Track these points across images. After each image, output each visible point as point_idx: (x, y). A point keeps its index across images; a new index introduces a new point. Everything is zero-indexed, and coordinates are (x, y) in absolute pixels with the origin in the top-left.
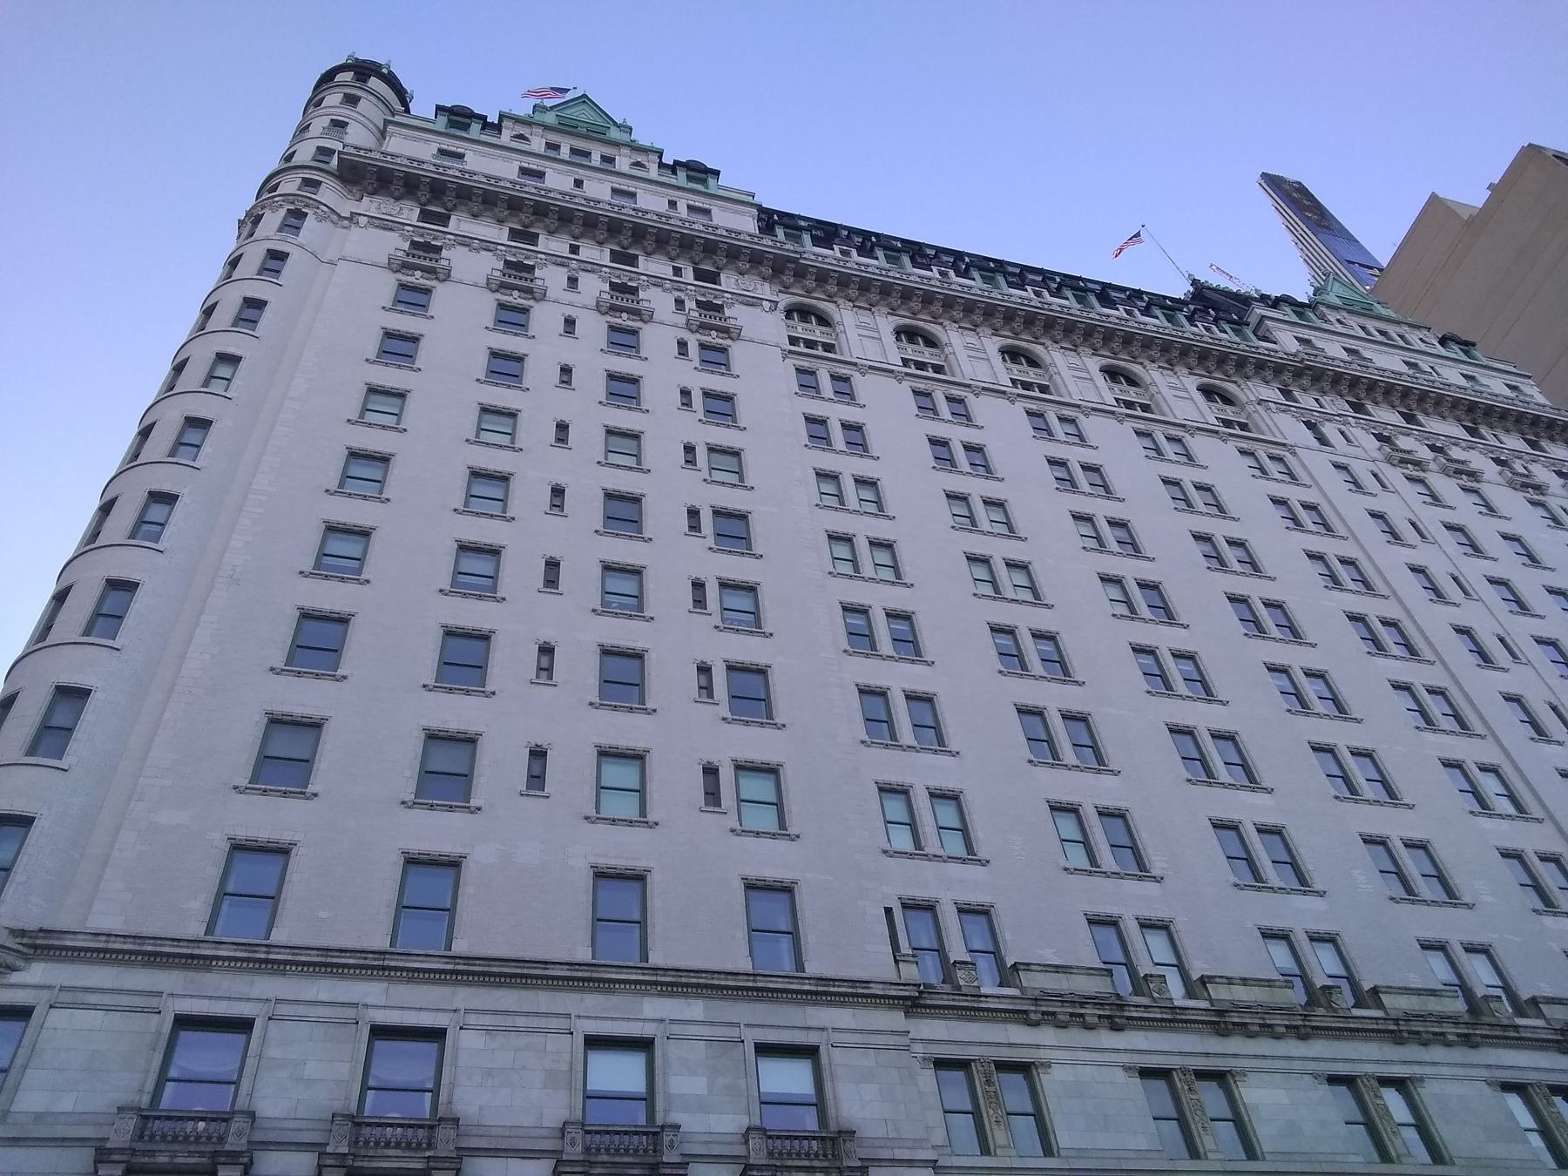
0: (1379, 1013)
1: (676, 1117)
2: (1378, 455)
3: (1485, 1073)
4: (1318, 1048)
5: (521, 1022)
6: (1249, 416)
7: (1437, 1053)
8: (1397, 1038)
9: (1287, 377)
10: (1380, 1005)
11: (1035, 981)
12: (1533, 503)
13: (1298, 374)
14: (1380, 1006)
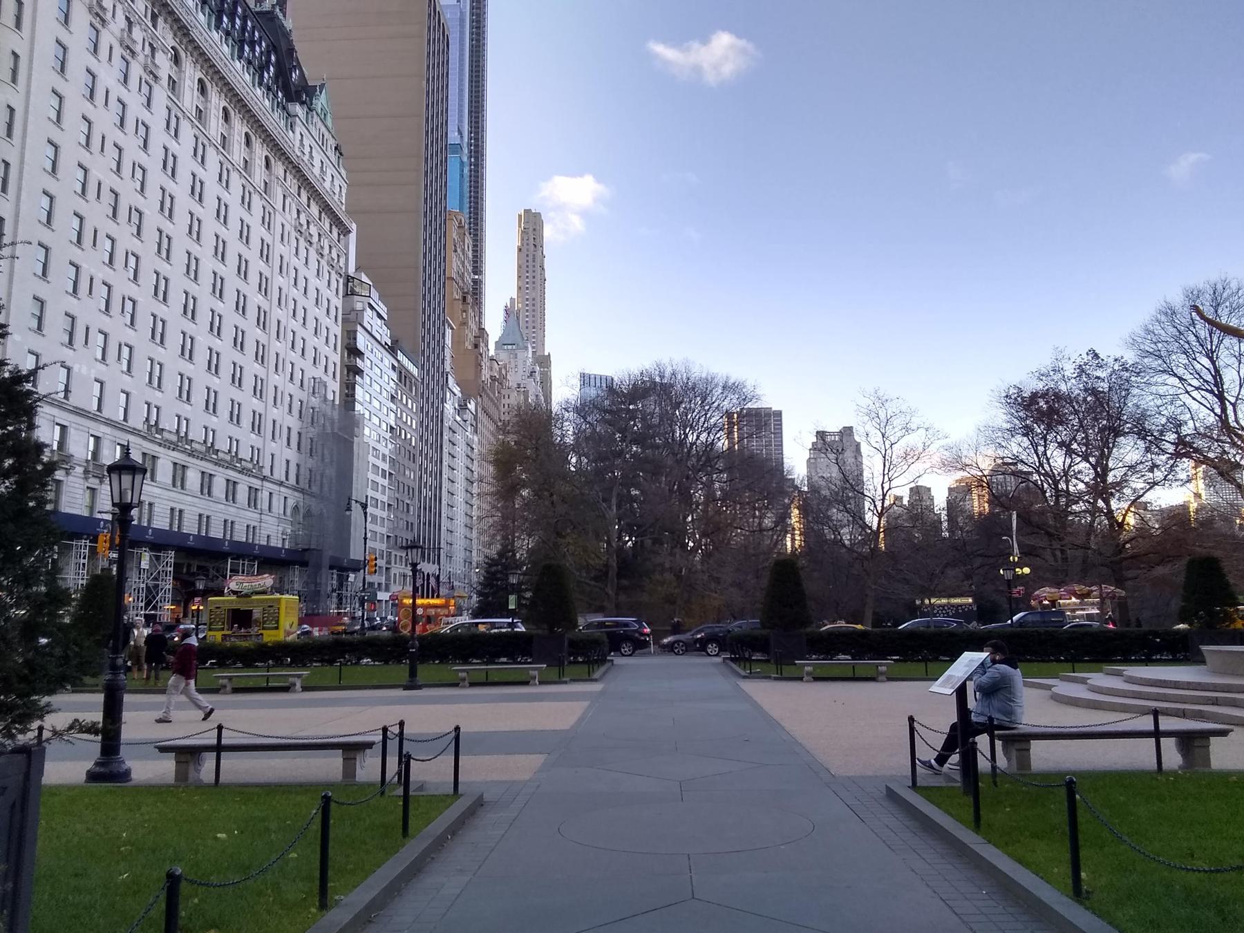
2: (293, 223)
3: (225, 476)
4: (203, 463)
5: (81, 427)
8: (216, 464)
9: (290, 166)
10: (217, 455)
11: (166, 435)
13: (295, 167)
14: (217, 455)
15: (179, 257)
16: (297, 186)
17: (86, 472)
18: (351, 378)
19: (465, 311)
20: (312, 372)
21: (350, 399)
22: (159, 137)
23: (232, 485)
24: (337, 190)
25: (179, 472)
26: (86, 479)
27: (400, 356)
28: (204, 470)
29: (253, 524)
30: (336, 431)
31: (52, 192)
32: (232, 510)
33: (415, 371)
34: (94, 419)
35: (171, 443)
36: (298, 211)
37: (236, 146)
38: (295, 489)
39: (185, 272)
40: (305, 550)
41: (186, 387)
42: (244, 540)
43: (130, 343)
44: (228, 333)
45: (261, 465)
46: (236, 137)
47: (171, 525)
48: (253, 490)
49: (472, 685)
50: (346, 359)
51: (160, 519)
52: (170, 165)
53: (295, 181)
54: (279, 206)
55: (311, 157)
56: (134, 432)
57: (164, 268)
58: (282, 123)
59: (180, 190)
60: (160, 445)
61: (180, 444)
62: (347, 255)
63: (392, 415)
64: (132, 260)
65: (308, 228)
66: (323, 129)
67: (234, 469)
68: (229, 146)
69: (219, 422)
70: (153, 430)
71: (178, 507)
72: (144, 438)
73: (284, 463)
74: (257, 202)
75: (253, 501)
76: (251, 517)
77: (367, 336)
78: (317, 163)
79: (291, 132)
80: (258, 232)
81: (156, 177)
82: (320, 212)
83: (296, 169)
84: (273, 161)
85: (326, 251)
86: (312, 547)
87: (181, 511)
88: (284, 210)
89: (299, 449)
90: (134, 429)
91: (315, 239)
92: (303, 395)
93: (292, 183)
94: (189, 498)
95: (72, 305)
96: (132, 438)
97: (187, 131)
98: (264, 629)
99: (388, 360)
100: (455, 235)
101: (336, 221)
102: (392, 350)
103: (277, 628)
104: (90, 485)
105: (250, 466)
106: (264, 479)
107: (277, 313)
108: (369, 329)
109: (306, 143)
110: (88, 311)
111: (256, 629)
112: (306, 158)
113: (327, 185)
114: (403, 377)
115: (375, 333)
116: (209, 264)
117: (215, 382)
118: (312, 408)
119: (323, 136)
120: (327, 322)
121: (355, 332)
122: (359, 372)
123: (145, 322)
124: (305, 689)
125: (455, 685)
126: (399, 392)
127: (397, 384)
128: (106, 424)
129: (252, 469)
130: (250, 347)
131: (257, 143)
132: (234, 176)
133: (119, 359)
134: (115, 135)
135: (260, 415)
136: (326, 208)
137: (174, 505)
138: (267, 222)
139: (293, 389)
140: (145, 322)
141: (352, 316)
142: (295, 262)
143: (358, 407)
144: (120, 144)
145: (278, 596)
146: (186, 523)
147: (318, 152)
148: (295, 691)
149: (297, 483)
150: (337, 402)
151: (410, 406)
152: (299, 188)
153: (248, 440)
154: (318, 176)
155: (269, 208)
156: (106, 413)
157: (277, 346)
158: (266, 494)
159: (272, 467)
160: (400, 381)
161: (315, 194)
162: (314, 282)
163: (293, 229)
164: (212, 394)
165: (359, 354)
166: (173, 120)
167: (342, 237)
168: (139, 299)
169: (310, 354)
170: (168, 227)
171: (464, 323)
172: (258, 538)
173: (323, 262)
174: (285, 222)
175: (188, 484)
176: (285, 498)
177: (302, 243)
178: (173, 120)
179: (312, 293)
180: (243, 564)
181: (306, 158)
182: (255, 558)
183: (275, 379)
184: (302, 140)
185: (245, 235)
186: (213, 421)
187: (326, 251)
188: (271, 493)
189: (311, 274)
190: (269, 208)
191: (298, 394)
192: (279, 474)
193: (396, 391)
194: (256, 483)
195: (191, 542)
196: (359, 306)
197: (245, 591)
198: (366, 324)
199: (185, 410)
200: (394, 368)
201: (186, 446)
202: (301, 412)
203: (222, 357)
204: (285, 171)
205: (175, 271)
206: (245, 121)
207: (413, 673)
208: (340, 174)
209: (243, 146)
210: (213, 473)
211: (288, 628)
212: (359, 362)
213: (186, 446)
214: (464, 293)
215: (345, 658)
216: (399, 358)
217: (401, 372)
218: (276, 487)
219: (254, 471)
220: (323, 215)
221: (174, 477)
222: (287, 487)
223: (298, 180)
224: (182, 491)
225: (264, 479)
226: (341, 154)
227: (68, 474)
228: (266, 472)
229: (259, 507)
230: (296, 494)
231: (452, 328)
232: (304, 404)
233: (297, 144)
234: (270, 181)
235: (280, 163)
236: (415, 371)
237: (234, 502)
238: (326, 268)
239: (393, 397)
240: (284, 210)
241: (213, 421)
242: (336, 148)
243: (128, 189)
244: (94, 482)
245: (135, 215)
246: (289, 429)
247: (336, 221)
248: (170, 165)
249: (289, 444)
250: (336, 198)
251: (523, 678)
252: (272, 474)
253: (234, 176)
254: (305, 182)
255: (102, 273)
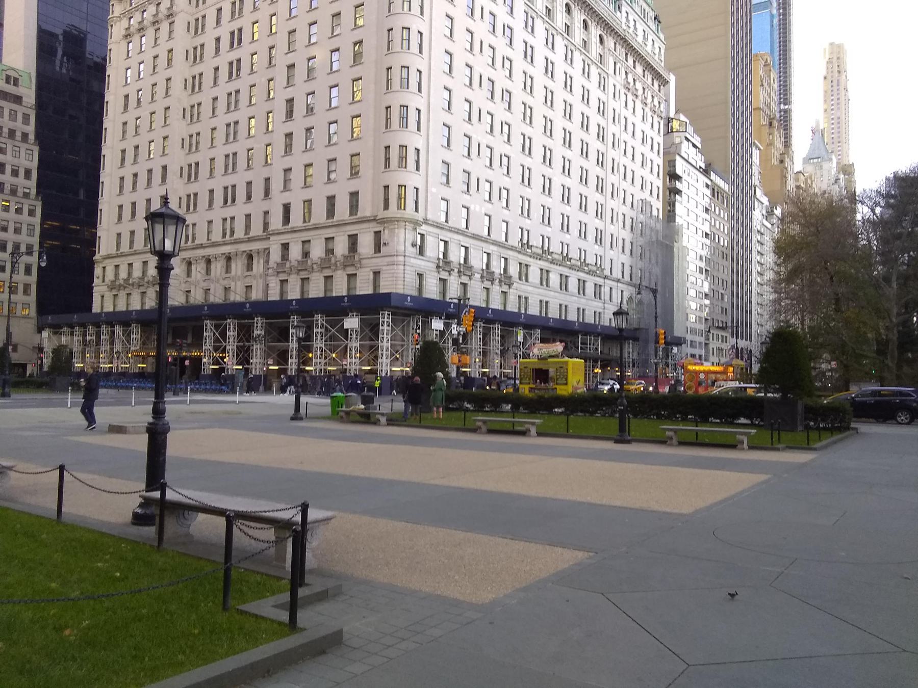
0: (569, 263)
1: (494, 270)
2: (622, 83)
4: (561, 268)
6: (604, 53)
7: (573, 272)
8: (570, 268)
9: (619, 38)
10: (570, 261)
12: (642, 108)
15: (538, 121)
16: (625, 54)
17: (482, 277)
18: (672, 197)
19: (771, 134)
20: (639, 196)
21: (671, 214)
22: (520, 35)
23: (582, 283)
24: (657, 51)
25: (545, 275)
26: (482, 282)
27: (713, 176)
28: (562, 273)
29: (598, 310)
30: (661, 238)
31: (450, 87)
32: (583, 301)
33: (725, 187)
34: (485, 241)
35: (538, 255)
36: (626, 73)
37: (577, 31)
38: (629, 284)
39: (543, 132)
40: (636, 329)
41: (547, 215)
42: (593, 322)
43: (507, 187)
44: (576, 173)
45: (603, 267)
46: (577, 24)
47: (541, 312)
48: (598, 287)
49: (682, 443)
50: (668, 183)
51: (533, 308)
52: (529, 54)
53: (623, 50)
54: (611, 71)
55: (635, 29)
56: (512, 248)
57: (528, 131)
58: (611, 7)
59: (537, 71)
60: (531, 257)
61: (544, 255)
62: (667, 101)
63: (707, 224)
64: (506, 128)
65: (634, 84)
66: (644, 5)
67: (583, 271)
68: (572, 32)
69: (572, 238)
70: (525, 246)
71: (545, 299)
72: (519, 252)
73: (620, 266)
74: (594, 71)
75: (598, 294)
76: (597, 305)
77: (685, 163)
78: (640, 33)
79: (618, 12)
80: (596, 94)
81: (520, 65)
82: (644, 71)
83: (624, 42)
84: (605, 37)
85: (649, 100)
86: (641, 327)
87: (547, 303)
88: (615, 73)
89: (631, 254)
90: (512, 246)
91: (640, 92)
92: (633, 214)
93: (621, 51)
94: (552, 293)
95: (467, 164)
96: (511, 253)
97: (540, 26)
98: (557, 384)
99: (703, 179)
100: (761, 73)
101: (657, 76)
102: (706, 172)
103: (566, 384)
104: (462, 281)
105: (595, 269)
106: (605, 277)
107: (611, 154)
108: (686, 158)
109: (631, 18)
110: (478, 167)
111: (551, 384)
112: (631, 31)
113: (649, 49)
114: (715, 192)
115: (691, 160)
116: (560, 123)
117: (567, 210)
118: (641, 223)
119: (644, 10)
120: (650, 155)
121: (675, 161)
122: (678, 192)
123: (516, 171)
124: (540, 434)
125: (663, 442)
126: (713, 205)
127: (711, 199)
128: (493, 244)
129: (597, 270)
130: (592, 182)
131: (592, 26)
132: (576, 54)
133: (500, 199)
134: (489, 39)
135: (601, 232)
136: (648, 67)
137: (542, 298)
138: (602, 86)
139: (626, 209)
140: (516, 171)
141: (672, 149)
142: (624, 112)
143: (678, 219)
144: (493, 44)
145: (566, 359)
146: (550, 310)
147: (641, 24)
148: (530, 436)
149: (631, 279)
150: (661, 216)
151: (722, 215)
152: (627, 54)
153: (593, 250)
154: (641, 43)
155: (603, 74)
156: (493, 237)
157: (612, 179)
158: (607, 289)
159: (611, 269)
160: (713, 196)
161: (639, 57)
162: (640, 126)
163: (622, 87)
164: (566, 219)
165: (678, 178)
166: (530, 20)
167: (662, 87)
168: (512, 155)
169: (638, 182)
170: (529, 100)
171: (771, 144)
172: (602, 320)
173: (647, 110)
174: (616, 84)
175: (551, 283)
176: (622, 291)
177: (630, 97)
178: (530, 20)
179: (639, 135)
180: (590, 340)
181: (631, 31)
182: (598, 335)
183: (612, 204)
184: (627, 17)
185: (586, 98)
186: (567, 238)
187: (649, 100)
188: (611, 288)
189: (638, 120)
190: (603, 74)
191: (630, 213)
192: (617, 274)
193: (710, 205)
194: (600, 281)
195: (551, 323)
196: (677, 141)
197: (544, 355)
198: (683, 154)
199: (547, 231)
200: (707, 186)
201: (549, 257)
202: (632, 226)
203: (571, 191)
204: (615, 44)
205: (536, 131)
206: (583, 11)
207: (622, 428)
208: (659, 38)
209: (582, 30)
210: (568, 275)
211: (575, 384)
212: (678, 185)
213: (549, 257)
214: (770, 119)
215: (602, 410)
216: (712, 178)
217: (713, 189)
218: (615, 284)
219: (598, 272)
220: (646, 72)
221: (541, 278)
222: (623, 283)
223: (625, 49)
224: (547, 288)
225: (605, 277)
226: (659, 22)
227: (470, 279)
228: (607, 272)
229: (603, 298)
230: (630, 288)
231: (759, 149)
232: (635, 221)
233: (624, 20)
234: (604, 53)
235: (611, 38)
236: (725, 187)
237: (584, 295)
238: (650, 113)
239: (707, 210)
240: (615, 73)
241: (567, 238)
242: (655, 18)
243: (500, 77)
244: (487, 284)
245: (506, 95)
246: (623, 240)
247: (657, 76)
248: (529, 54)
249: (623, 251)
250: (656, 57)
251: (730, 441)
252: (611, 274)
253: (576, 54)
254: (630, 49)
255: (486, 140)
